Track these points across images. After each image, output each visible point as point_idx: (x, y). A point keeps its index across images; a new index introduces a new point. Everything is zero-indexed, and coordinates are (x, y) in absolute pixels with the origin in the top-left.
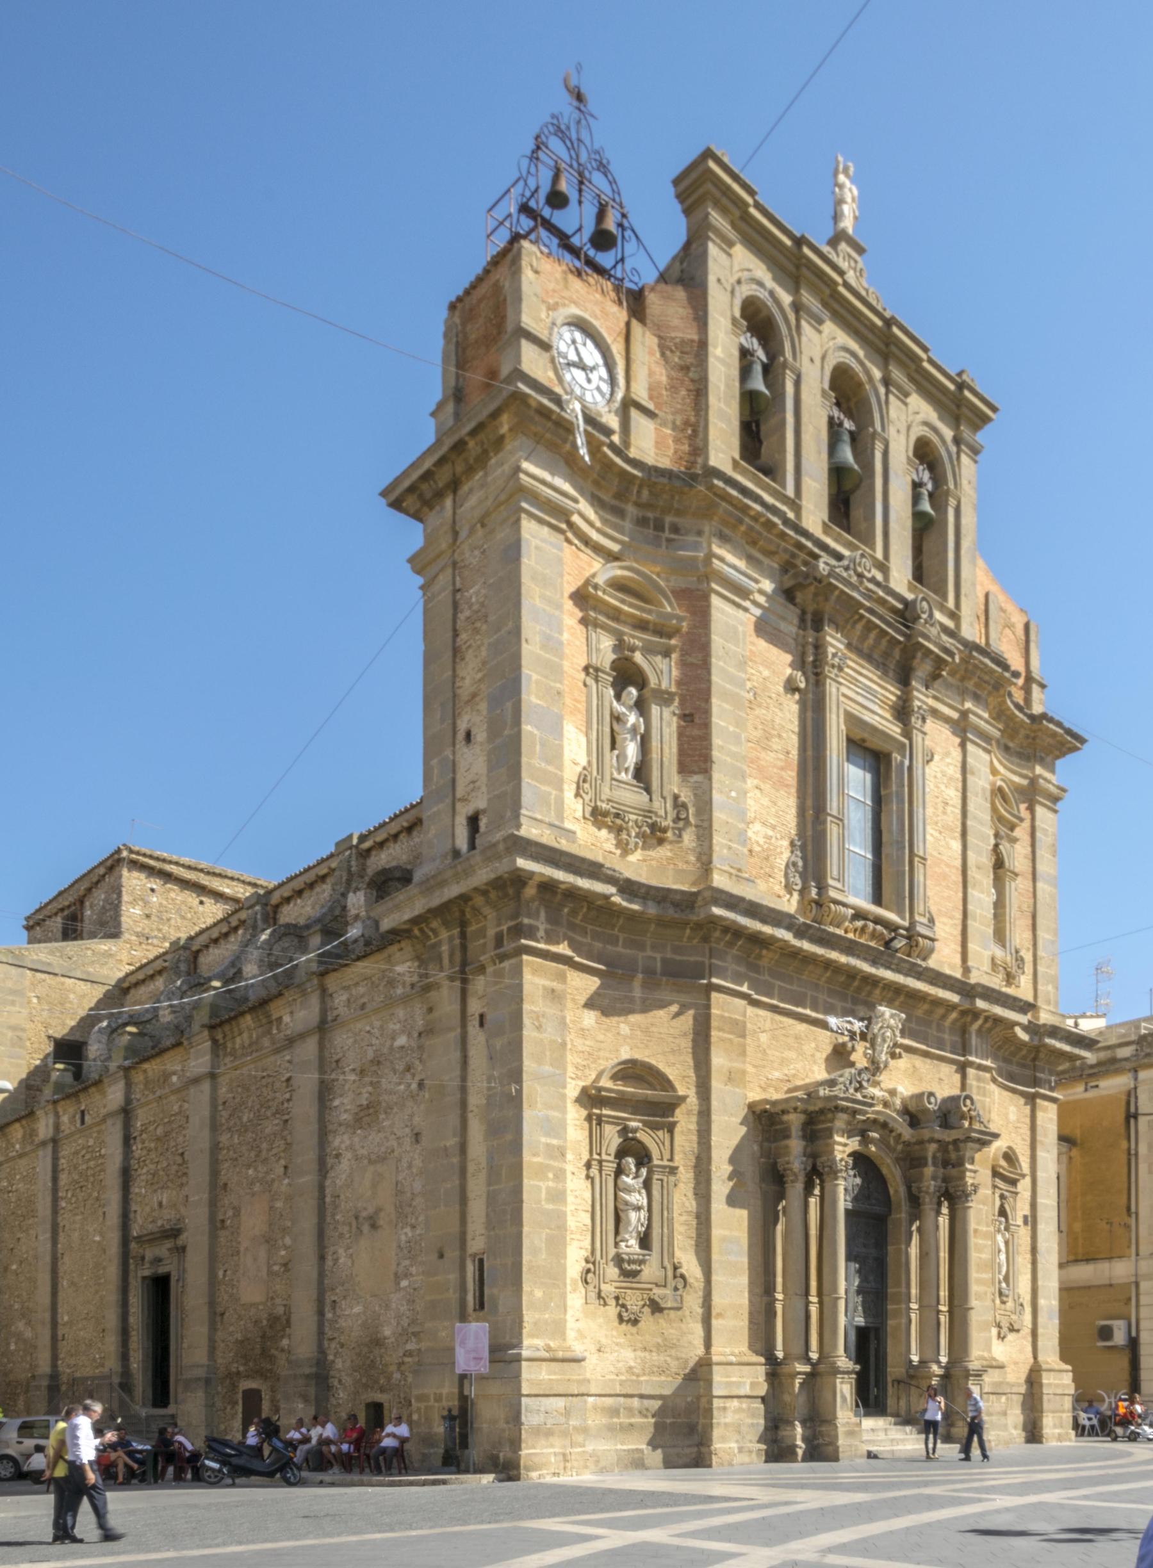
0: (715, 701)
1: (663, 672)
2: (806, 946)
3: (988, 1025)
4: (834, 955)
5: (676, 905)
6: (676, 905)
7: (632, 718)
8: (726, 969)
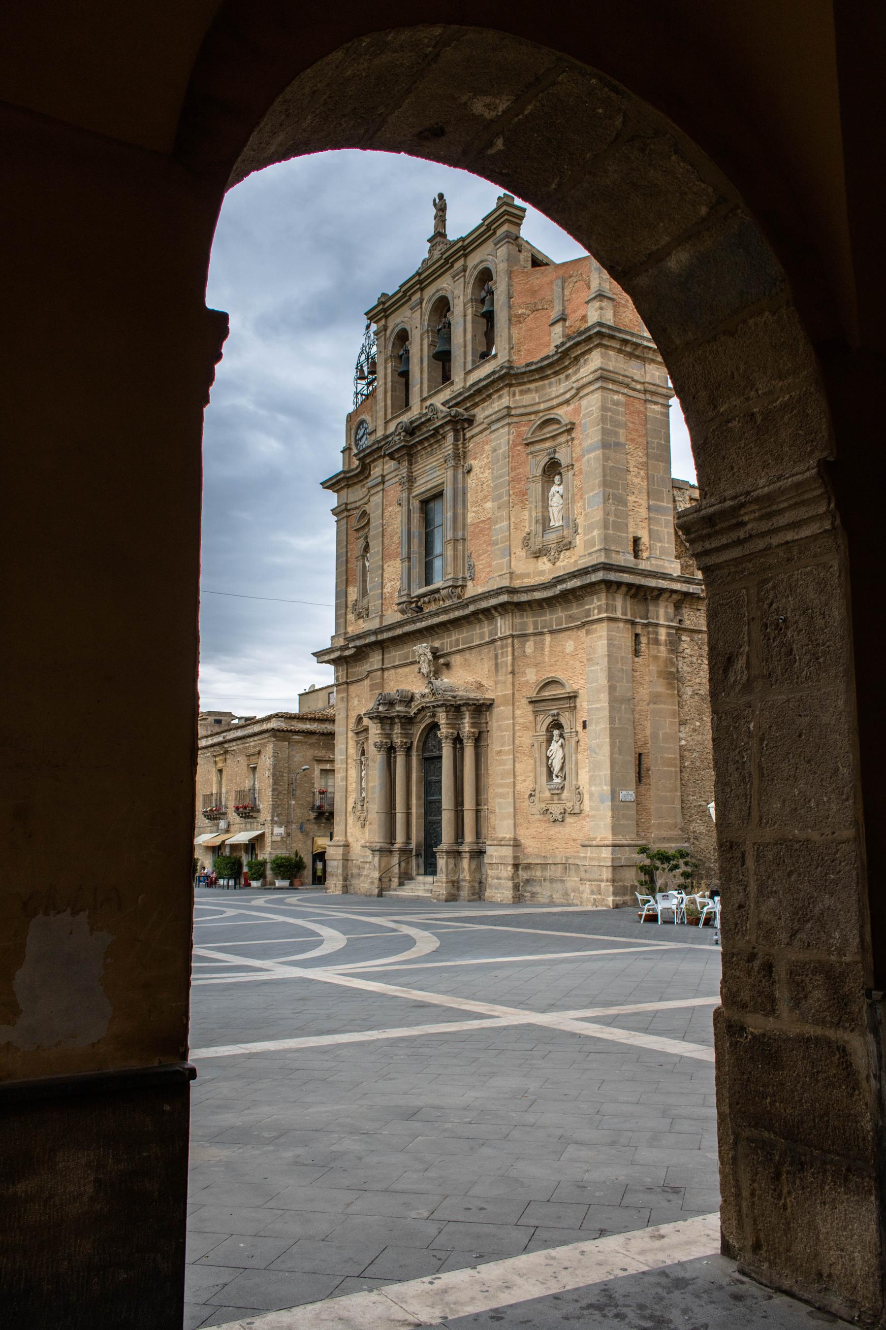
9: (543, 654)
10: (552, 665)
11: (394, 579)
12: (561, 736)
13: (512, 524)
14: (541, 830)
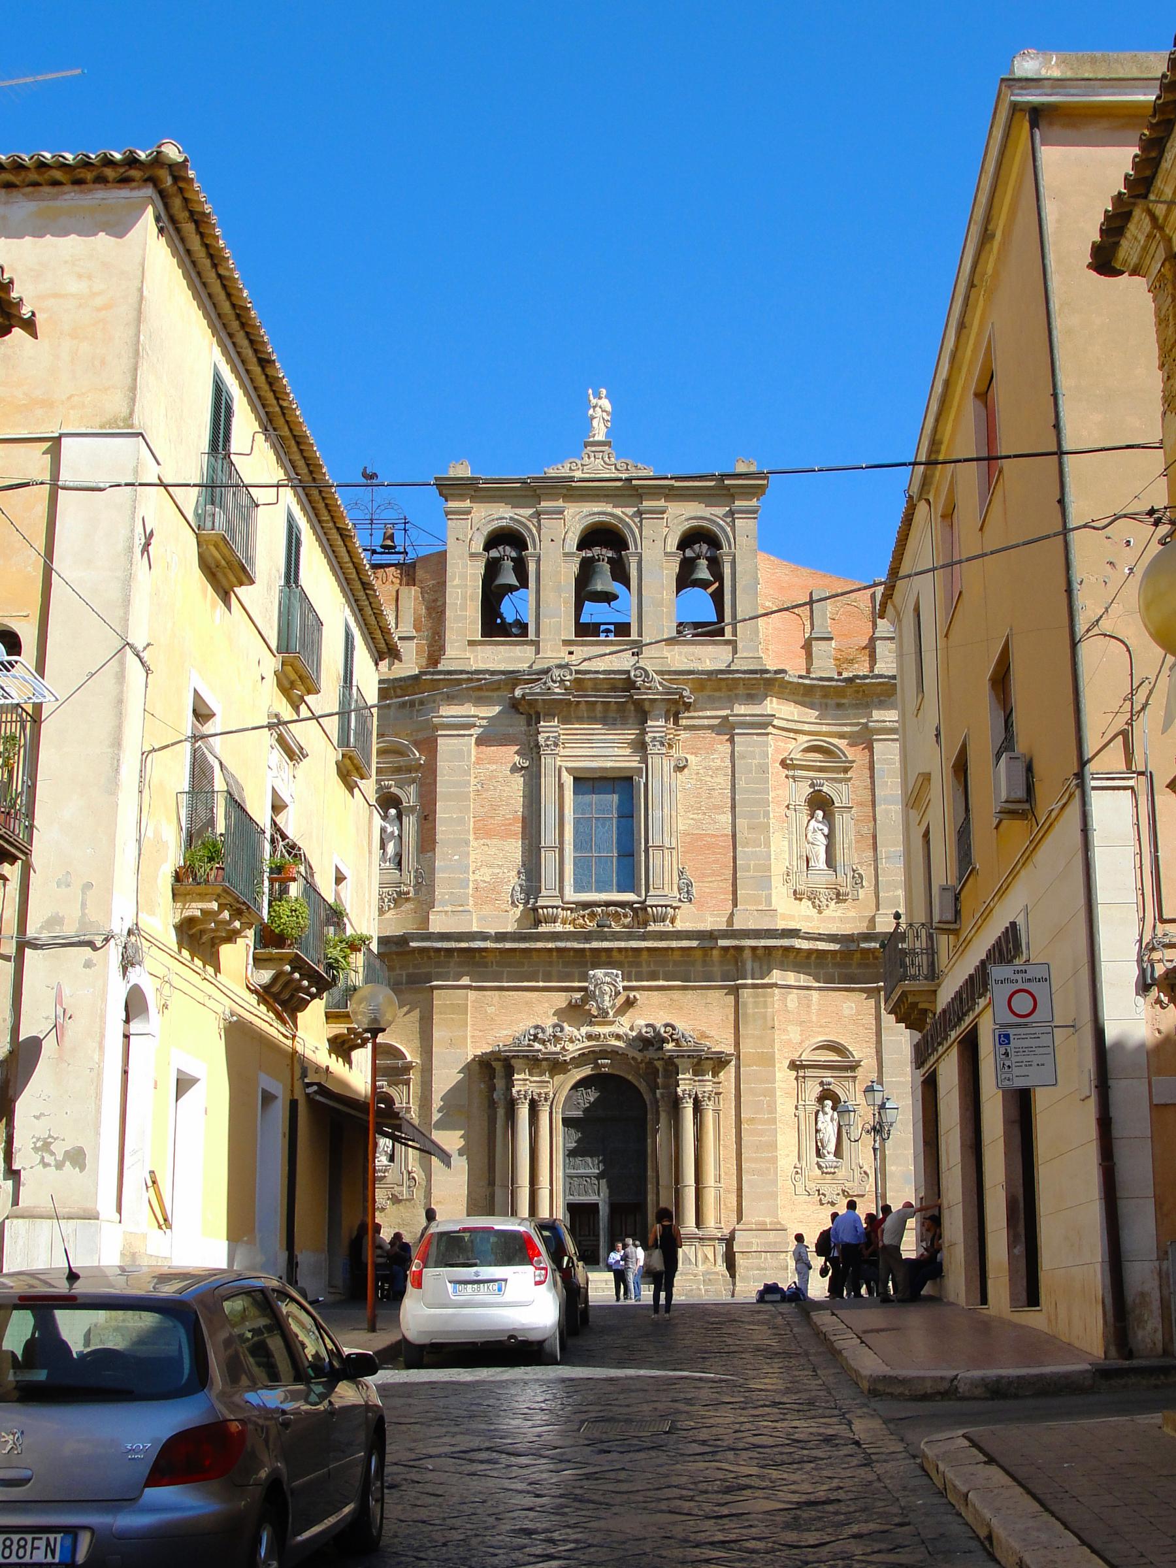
0: (439, 805)
1: (410, 796)
2: (508, 945)
3: (759, 952)
4: (540, 945)
5: (396, 944)
6: (396, 944)
7: (392, 829)
8: (448, 972)
9: (809, 1013)
10: (821, 1027)
11: (500, 866)
12: (834, 1109)
13: (772, 853)
14: (809, 1213)
